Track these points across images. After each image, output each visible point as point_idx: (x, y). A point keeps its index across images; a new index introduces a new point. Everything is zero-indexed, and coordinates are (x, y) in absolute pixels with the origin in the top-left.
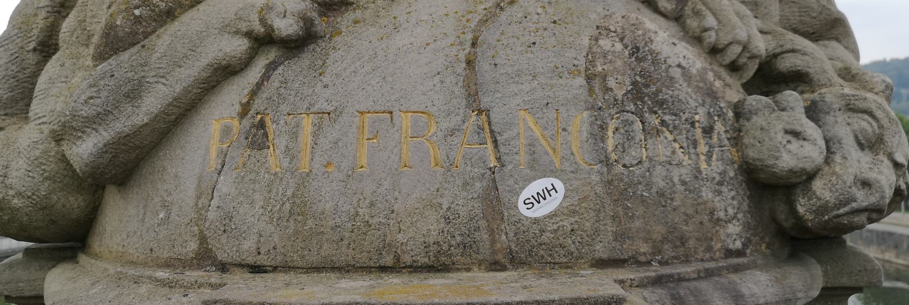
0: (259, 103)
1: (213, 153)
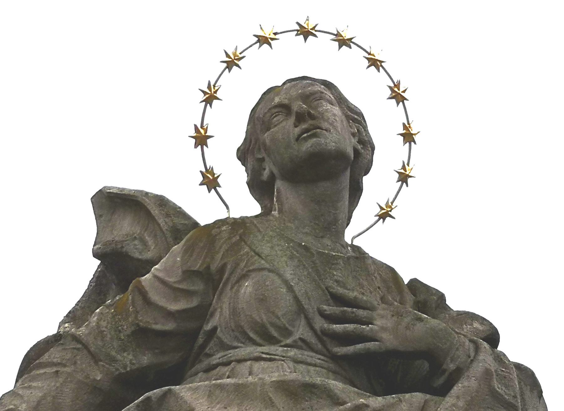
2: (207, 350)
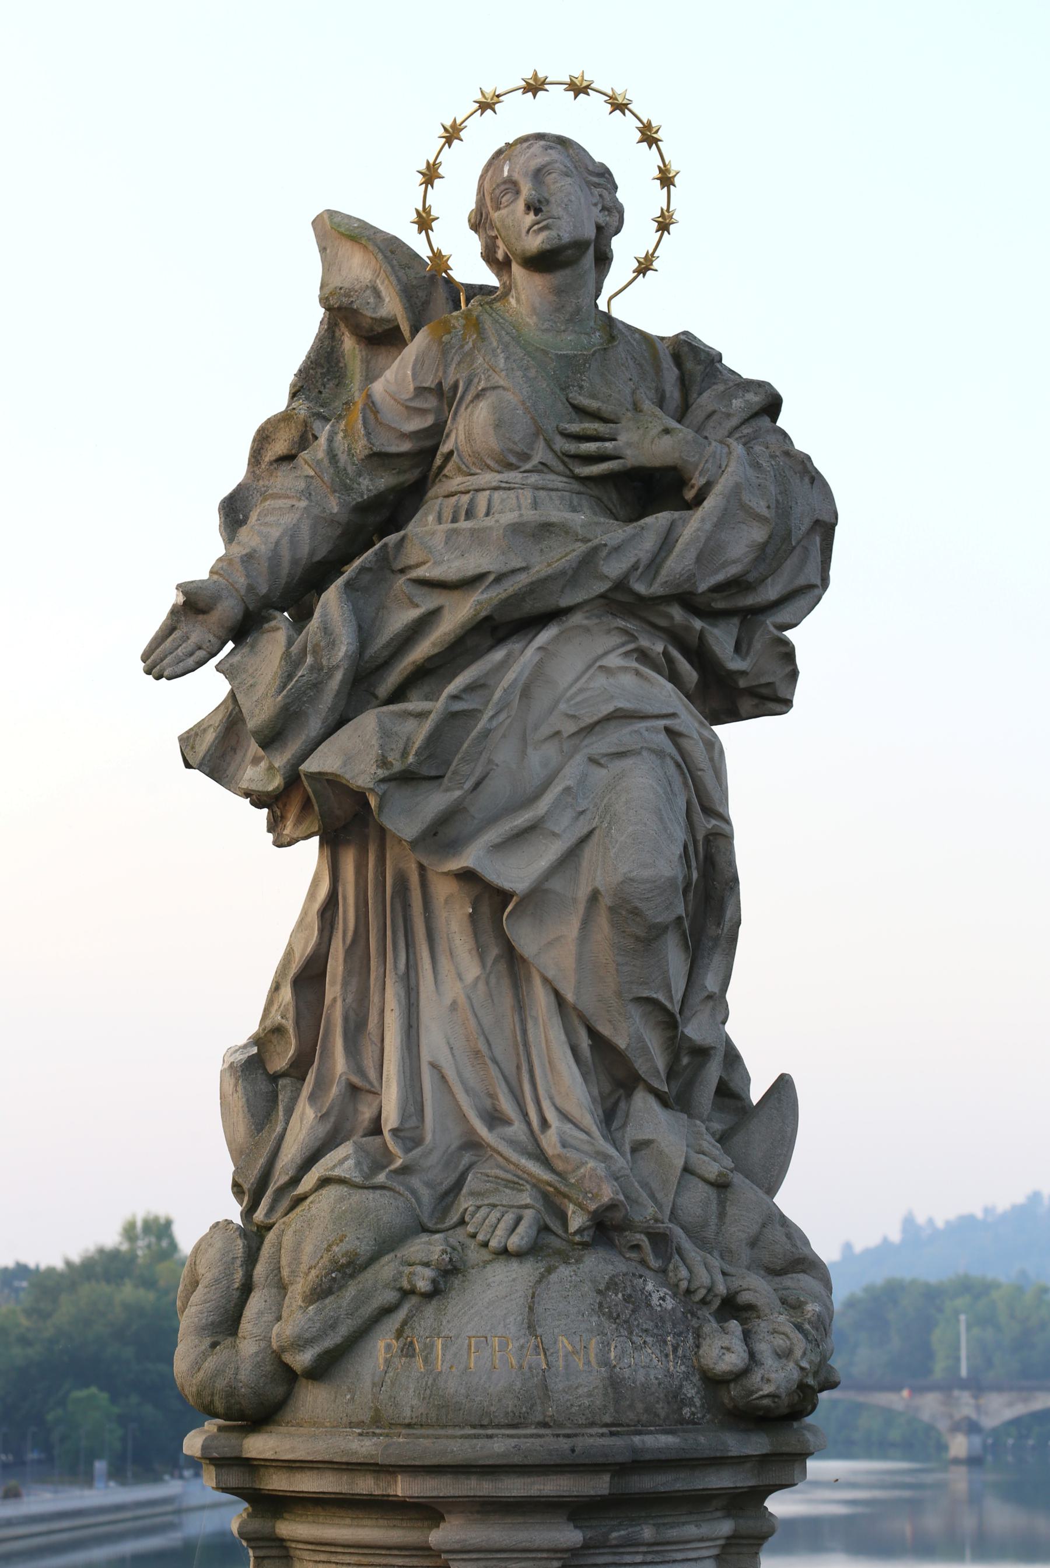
0: (408, 1332)
1: (381, 1361)
2: (446, 471)
